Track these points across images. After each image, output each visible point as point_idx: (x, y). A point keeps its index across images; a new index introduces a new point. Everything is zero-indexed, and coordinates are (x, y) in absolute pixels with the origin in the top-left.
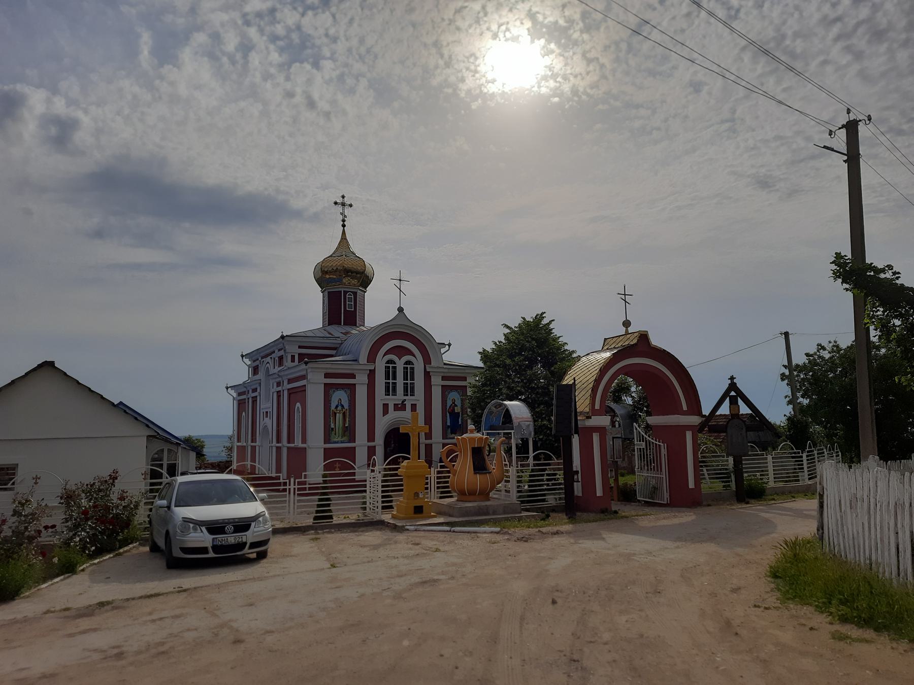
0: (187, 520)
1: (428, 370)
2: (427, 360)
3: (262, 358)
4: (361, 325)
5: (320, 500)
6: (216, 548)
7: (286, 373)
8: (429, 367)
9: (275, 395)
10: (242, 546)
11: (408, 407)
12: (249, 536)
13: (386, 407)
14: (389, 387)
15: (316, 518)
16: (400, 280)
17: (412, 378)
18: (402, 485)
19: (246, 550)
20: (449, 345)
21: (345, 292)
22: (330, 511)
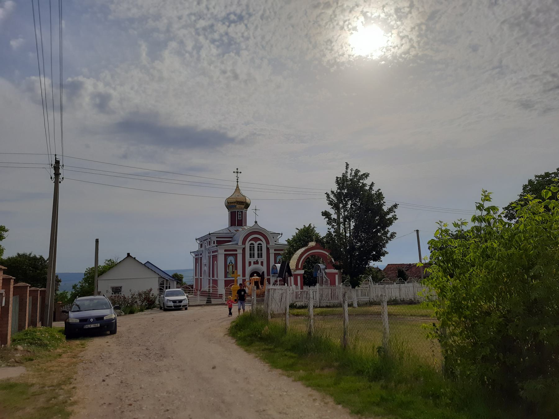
0: (168, 300)
1: (268, 247)
2: (268, 243)
3: (204, 241)
4: (244, 226)
5: (208, 299)
6: (174, 306)
7: (211, 249)
8: (269, 246)
9: (208, 257)
10: (180, 306)
11: (260, 263)
12: (182, 304)
13: (250, 263)
14: (251, 254)
15: (207, 302)
16: (256, 210)
17: (261, 251)
18: (231, 293)
19: (181, 307)
20: (282, 234)
21: (238, 212)
22: (211, 300)
